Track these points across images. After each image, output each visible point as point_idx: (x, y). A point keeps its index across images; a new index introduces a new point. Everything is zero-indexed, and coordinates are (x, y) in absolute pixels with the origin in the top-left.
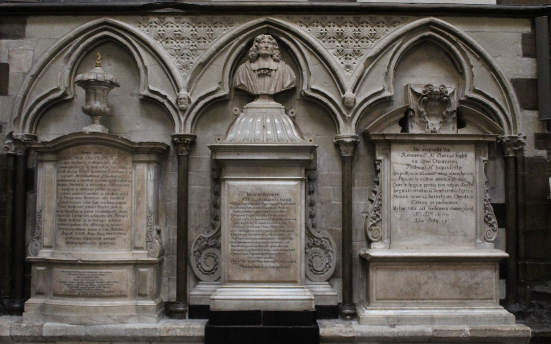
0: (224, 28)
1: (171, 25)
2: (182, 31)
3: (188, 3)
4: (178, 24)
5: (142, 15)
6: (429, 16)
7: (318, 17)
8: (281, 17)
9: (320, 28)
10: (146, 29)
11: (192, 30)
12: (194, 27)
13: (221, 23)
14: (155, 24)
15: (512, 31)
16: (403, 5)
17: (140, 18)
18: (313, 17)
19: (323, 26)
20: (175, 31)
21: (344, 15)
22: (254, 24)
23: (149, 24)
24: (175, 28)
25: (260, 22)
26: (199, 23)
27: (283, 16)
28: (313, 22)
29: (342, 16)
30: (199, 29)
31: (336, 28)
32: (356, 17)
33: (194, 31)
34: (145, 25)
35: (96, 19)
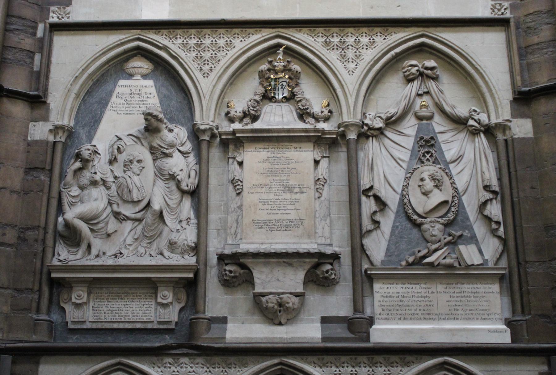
0: (238, 369)
1: (185, 365)
2: (196, 372)
3: (203, 344)
4: (192, 365)
5: (157, 355)
6: (443, 355)
7: (331, 358)
8: (296, 358)
9: (334, 369)
10: (159, 370)
11: (206, 371)
12: (208, 368)
13: (236, 365)
14: (169, 365)
15: (528, 370)
16: (415, 345)
17: (154, 359)
18: (327, 358)
19: (337, 367)
20: (190, 372)
21: (358, 355)
22: (268, 365)
23: (163, 365)
24: (189, 369)
25: (274, 363)
26: (214, 364)
27: (297, 357)
28: (327, 363)
29: (356, 356)
30: (213, 370)
31: (350, 369)
32: (369, 358)
33: (208, 372)
34: (159, 365)
35: (110, 359)
